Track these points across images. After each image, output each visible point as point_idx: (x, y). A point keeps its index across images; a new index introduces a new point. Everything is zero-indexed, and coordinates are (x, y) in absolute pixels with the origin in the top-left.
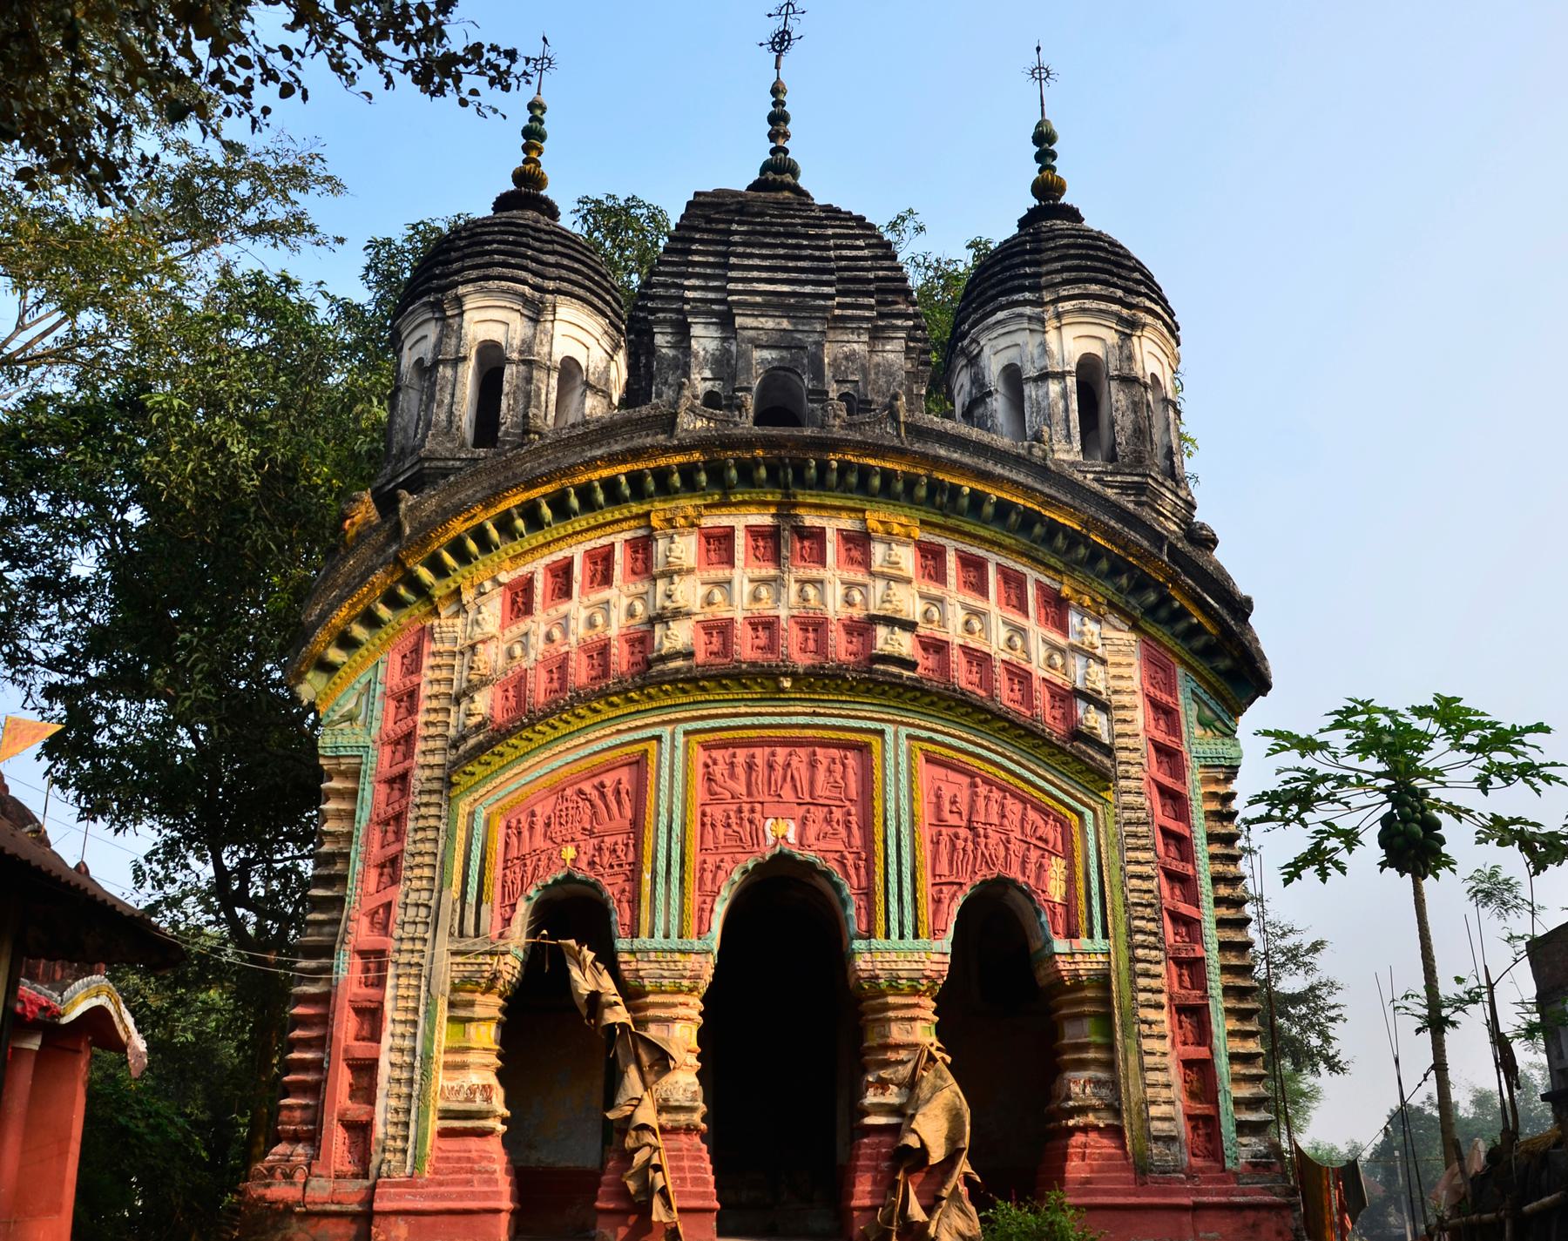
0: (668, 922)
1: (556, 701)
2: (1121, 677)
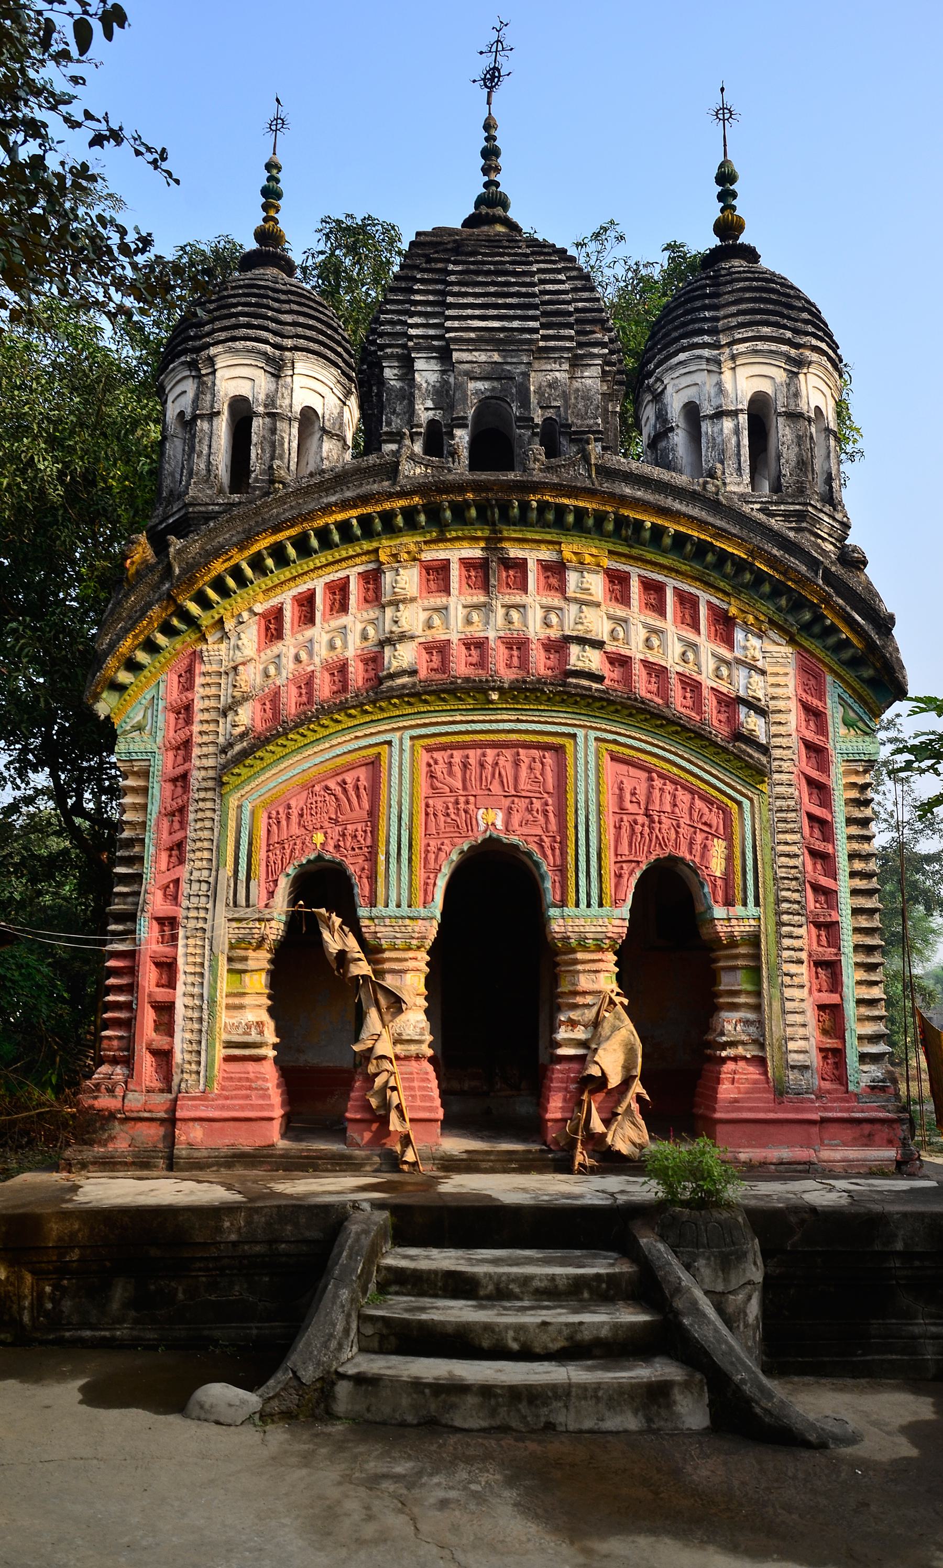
0: (399, 894)
1: (305, 713)
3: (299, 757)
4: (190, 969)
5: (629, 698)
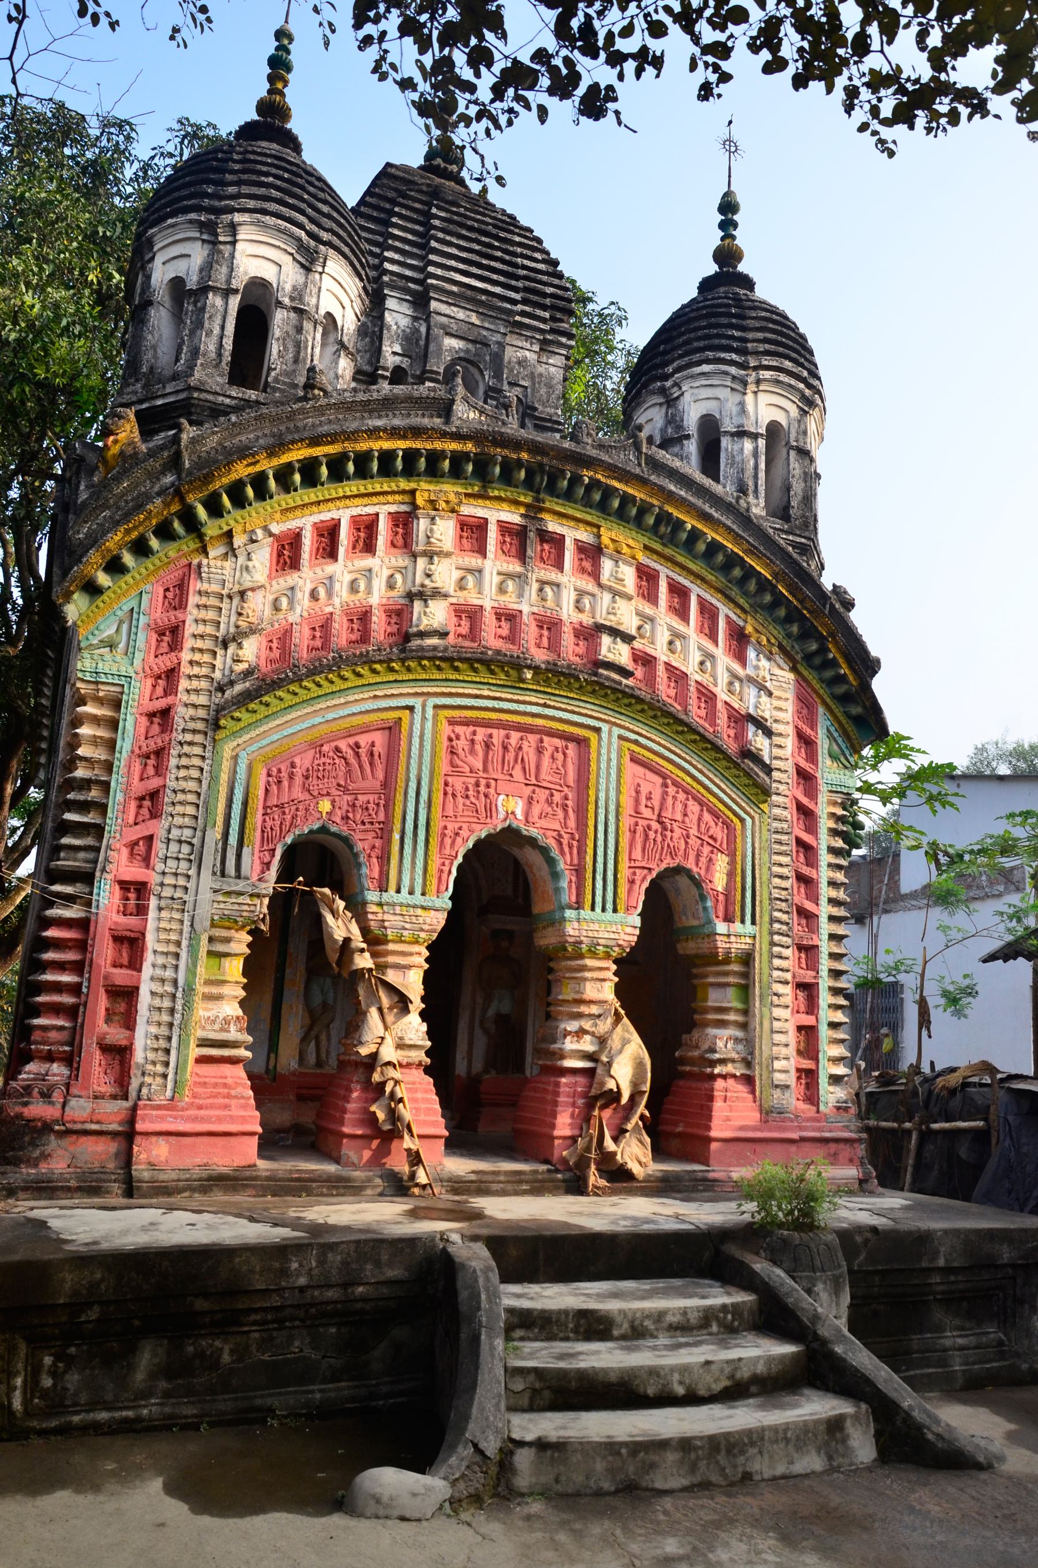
0: (412, 880)
1: (320, 660)
2: (780, 709)
3: (309, 710)
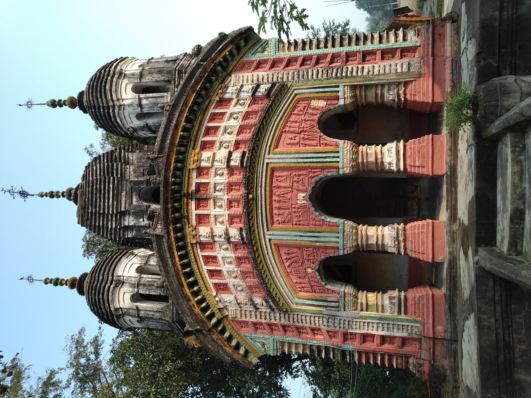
2: (247, 79)
4: (366, 328)
5: (252, 141)
